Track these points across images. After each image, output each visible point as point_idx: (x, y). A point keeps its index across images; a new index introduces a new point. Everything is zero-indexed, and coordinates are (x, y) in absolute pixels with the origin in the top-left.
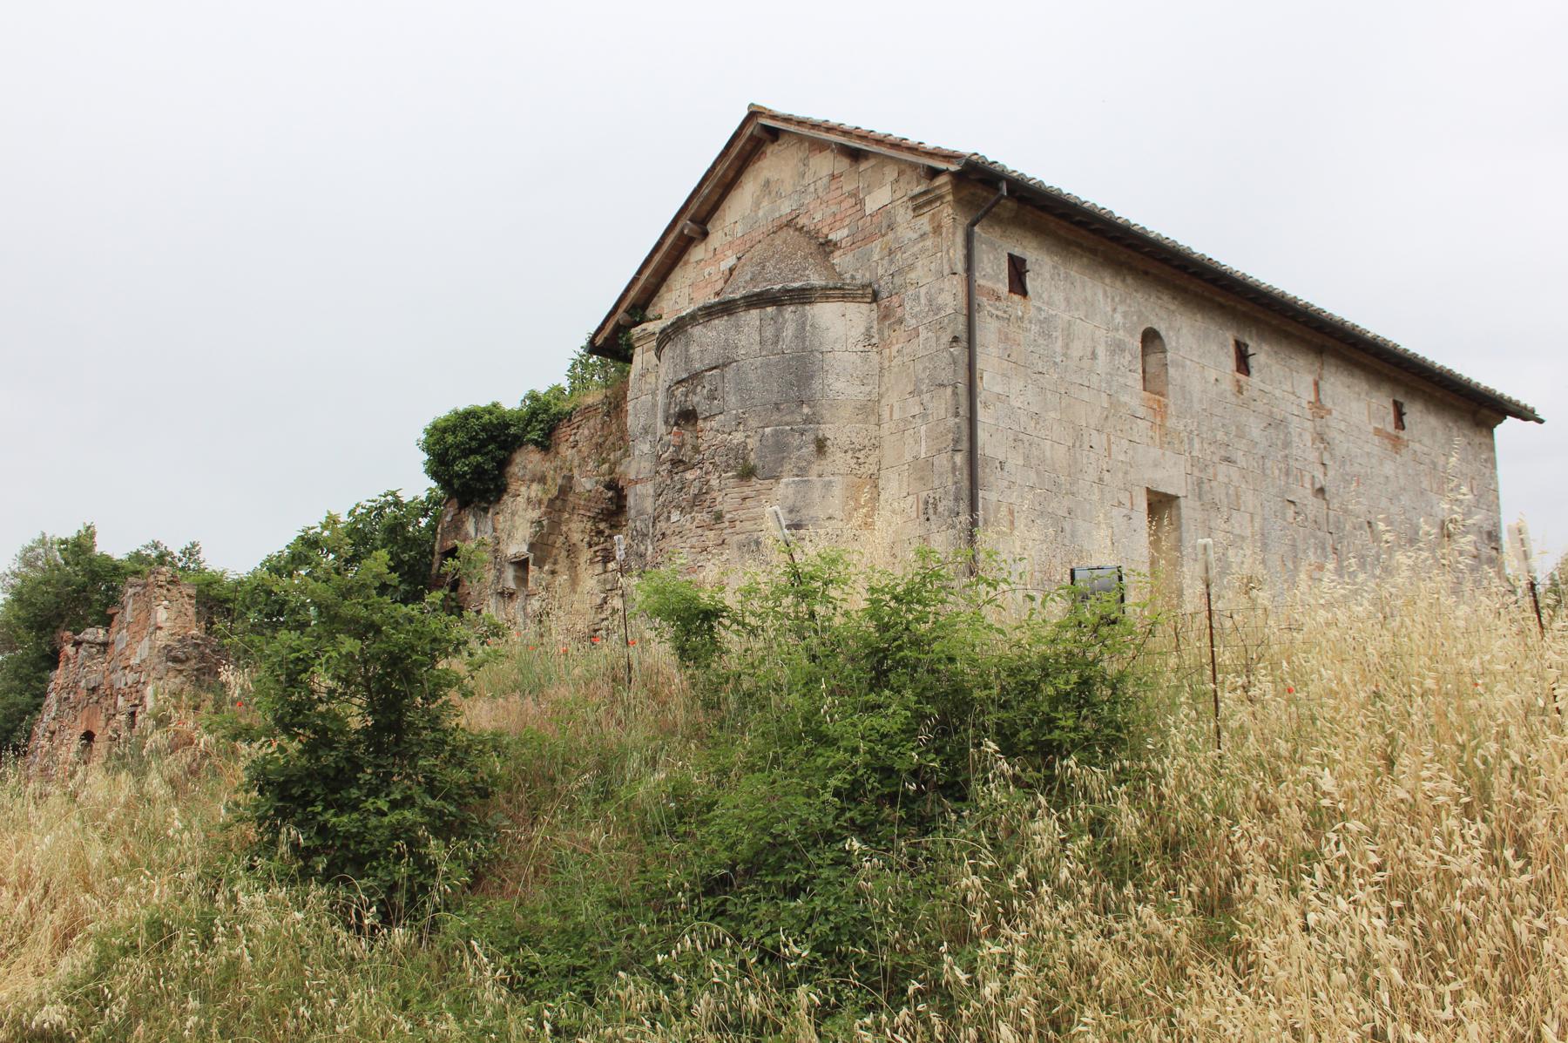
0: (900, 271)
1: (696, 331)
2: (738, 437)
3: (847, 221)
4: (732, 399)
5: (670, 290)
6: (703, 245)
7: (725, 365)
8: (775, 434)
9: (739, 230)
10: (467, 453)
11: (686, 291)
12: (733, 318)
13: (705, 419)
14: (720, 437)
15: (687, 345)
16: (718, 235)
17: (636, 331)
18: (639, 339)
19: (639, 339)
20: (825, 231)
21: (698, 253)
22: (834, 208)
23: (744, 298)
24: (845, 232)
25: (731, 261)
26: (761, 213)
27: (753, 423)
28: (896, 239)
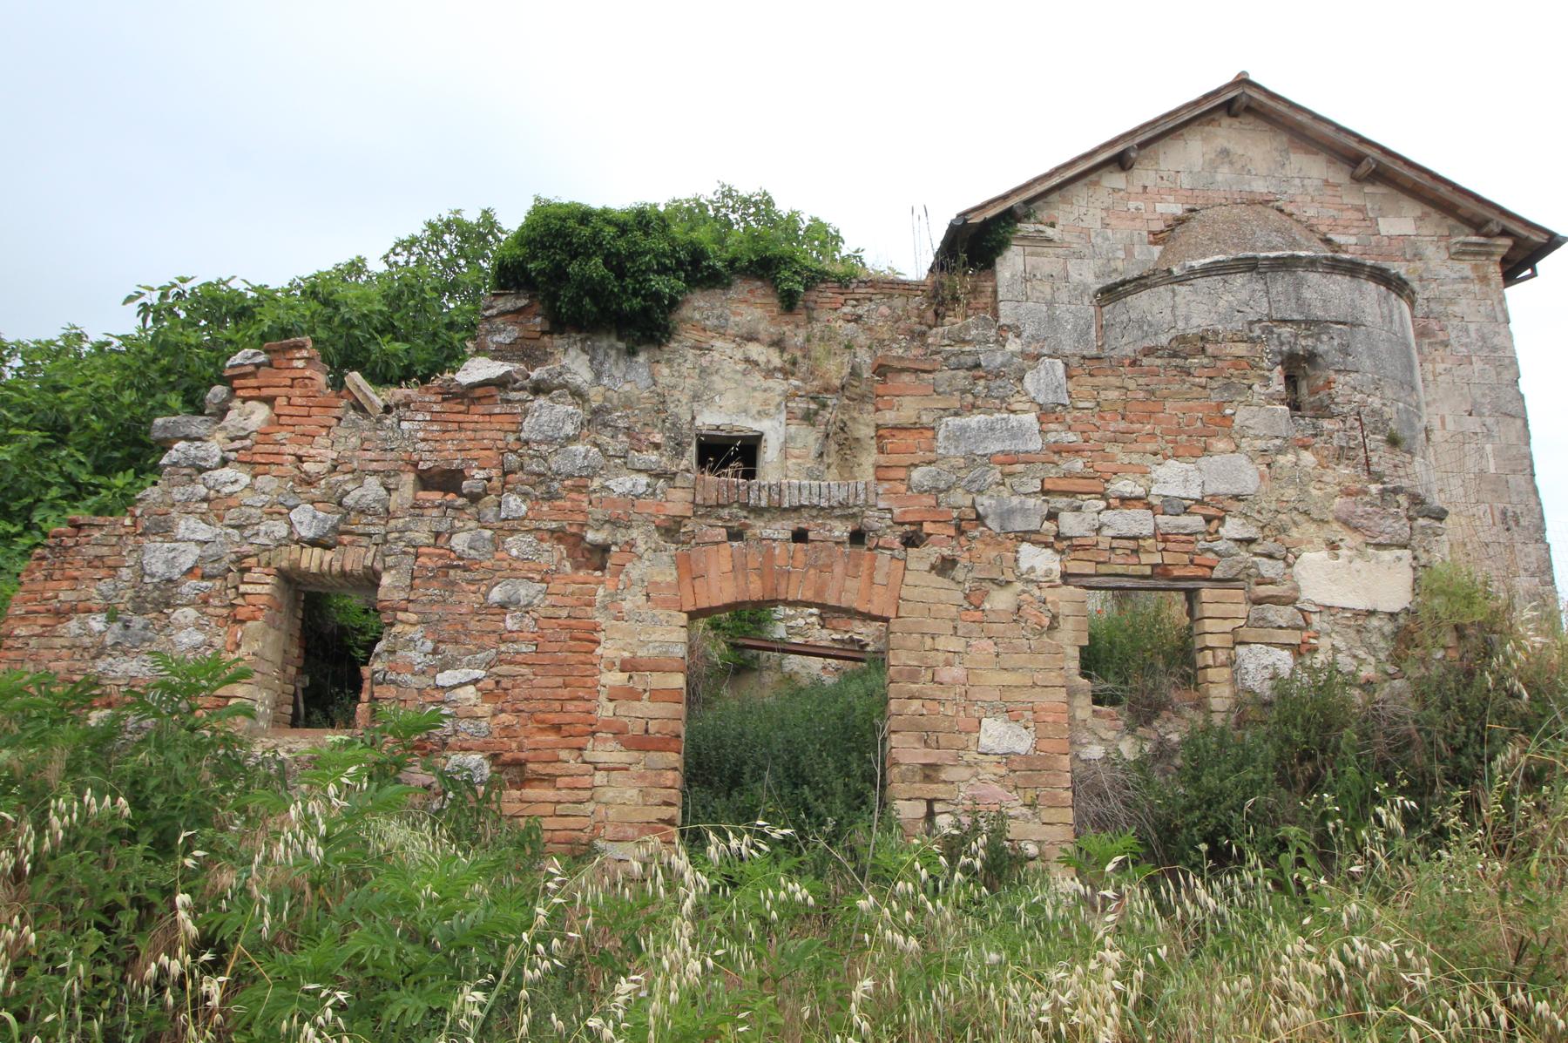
0: (1438, 300)
1: (1313, 278)
2: (1376, 402)
3: (1355, 231)
4: (1367, 363)
5: (1065, 201)
6: (1123, 175)
7: (1353, 325)
8: (1407, 411)
9: (1186, 181)
10: (663, 270)
11: (1100, 214)
12: (1355, 283)
13: (1338, 371)
14: (1358, 397)
15: (1298, 285)
16: (1144, 175)
17: (1026, 227)
18: (1024, 238)
19: (1024, 238)
20: (1323, 228)
21: (1116, 180)
22: (1333, 212)
23: (1372, 267)
24: (1353, 240)
25: (1178, 210)
26: (1219, 177)
27: (1389, 393)
28: (1427, 269)
